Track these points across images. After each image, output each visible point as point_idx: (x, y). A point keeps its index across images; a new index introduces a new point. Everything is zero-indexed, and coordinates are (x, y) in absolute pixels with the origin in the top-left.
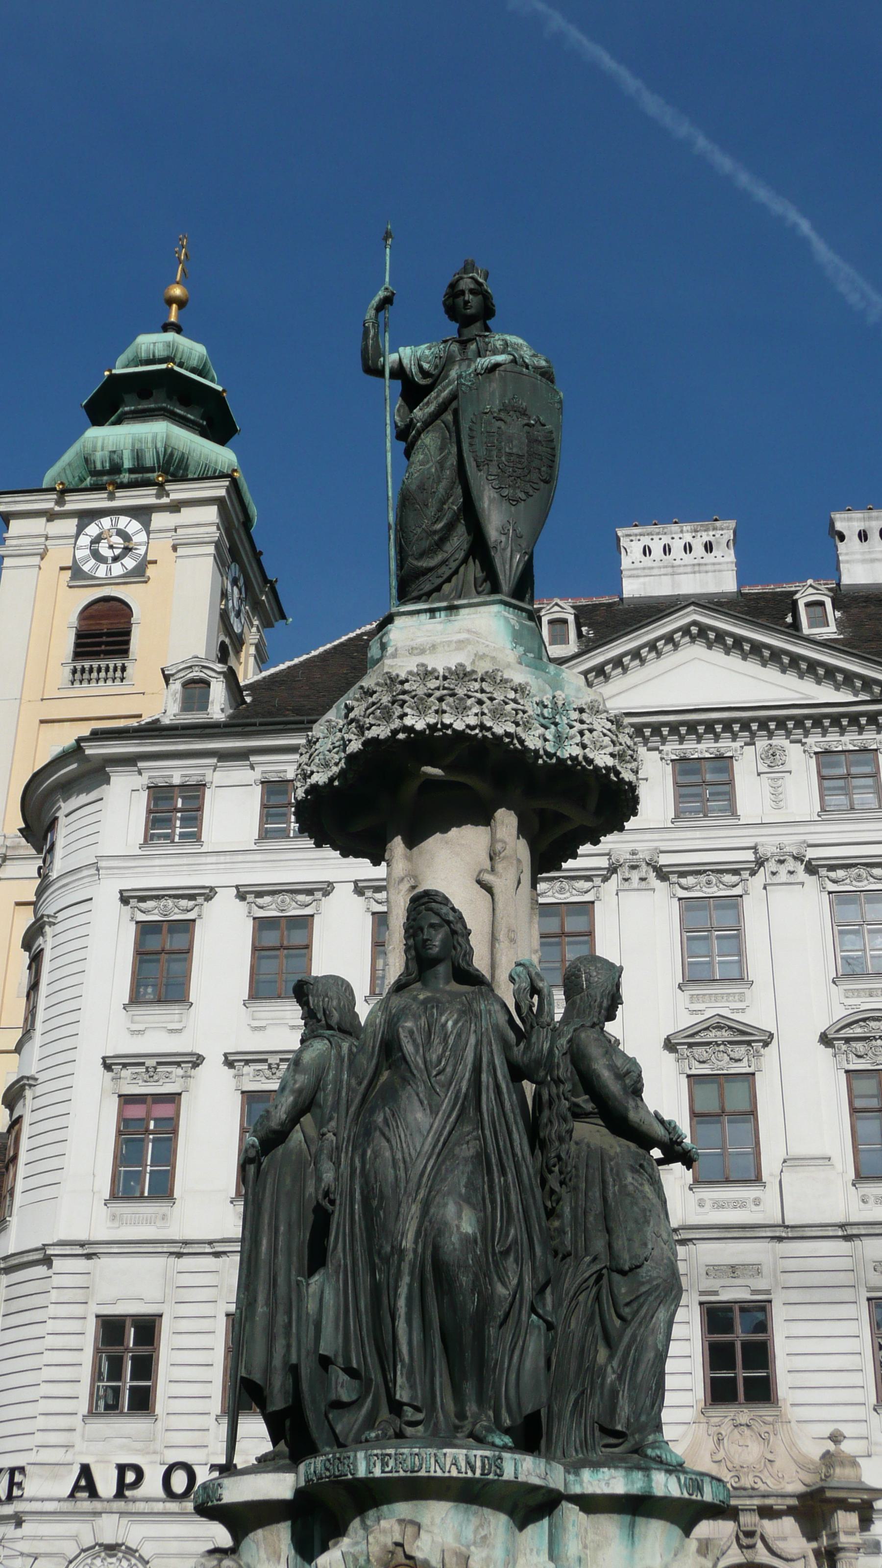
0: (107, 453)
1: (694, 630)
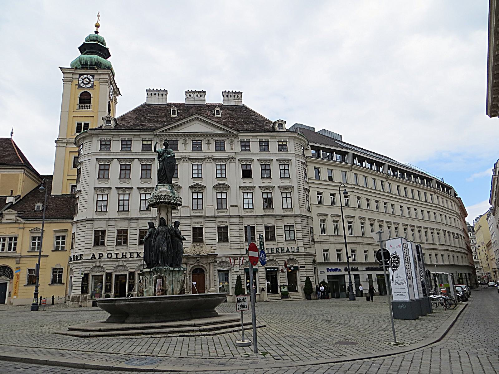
1: (197, 118)
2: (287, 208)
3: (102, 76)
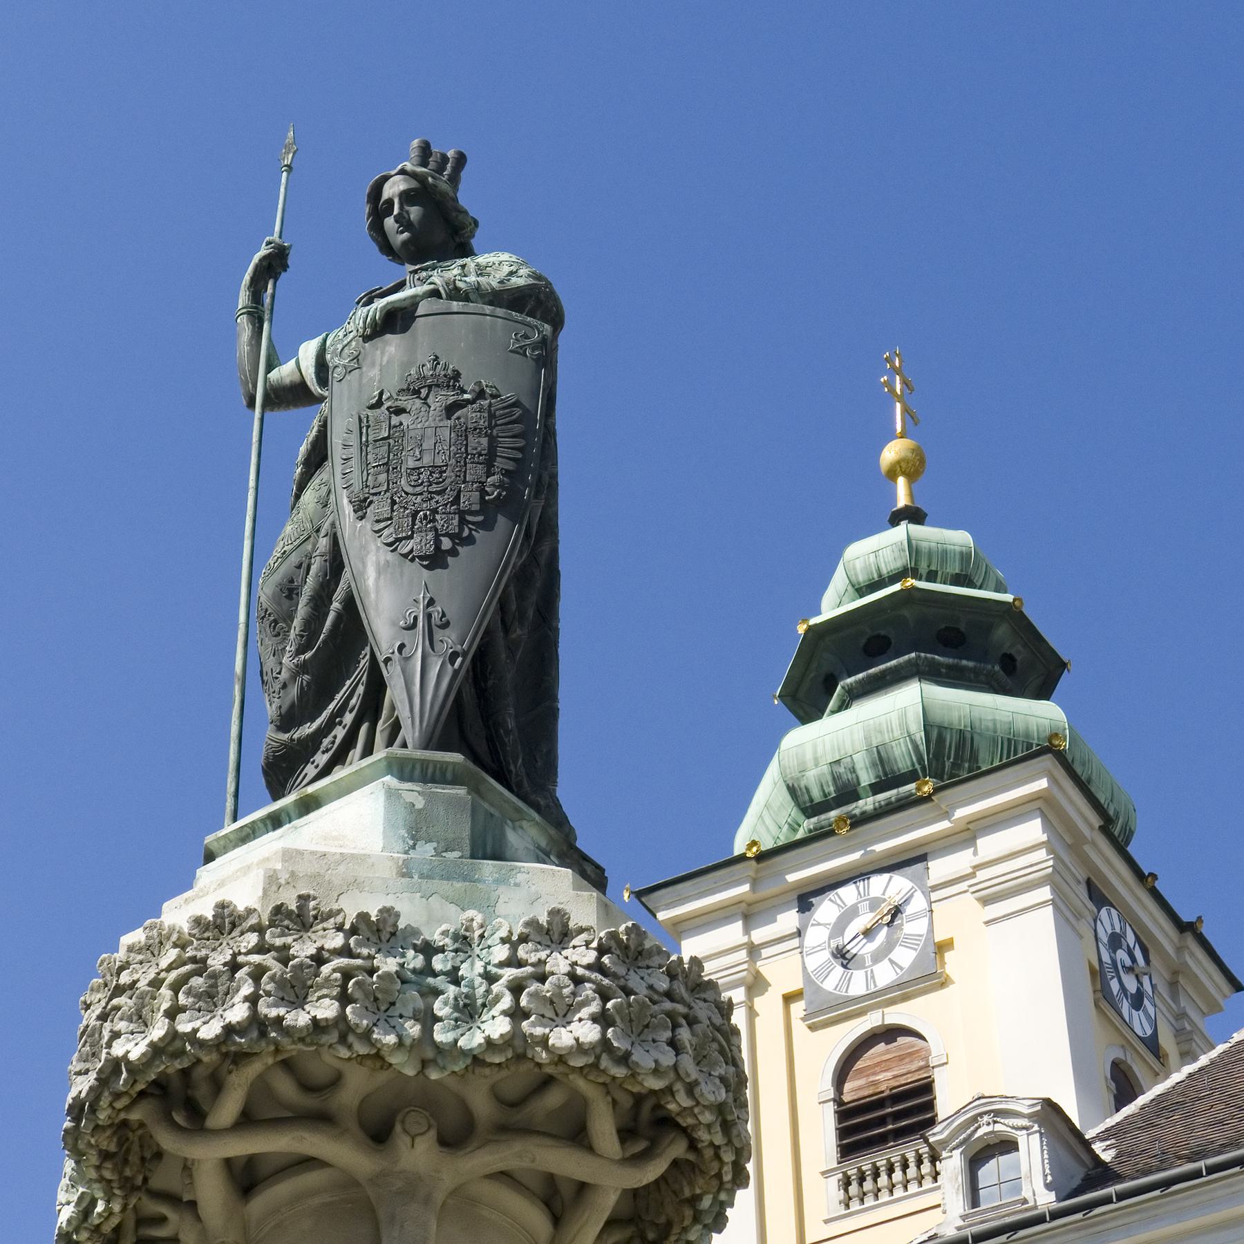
0: (825, 769)
3: (991, 845)
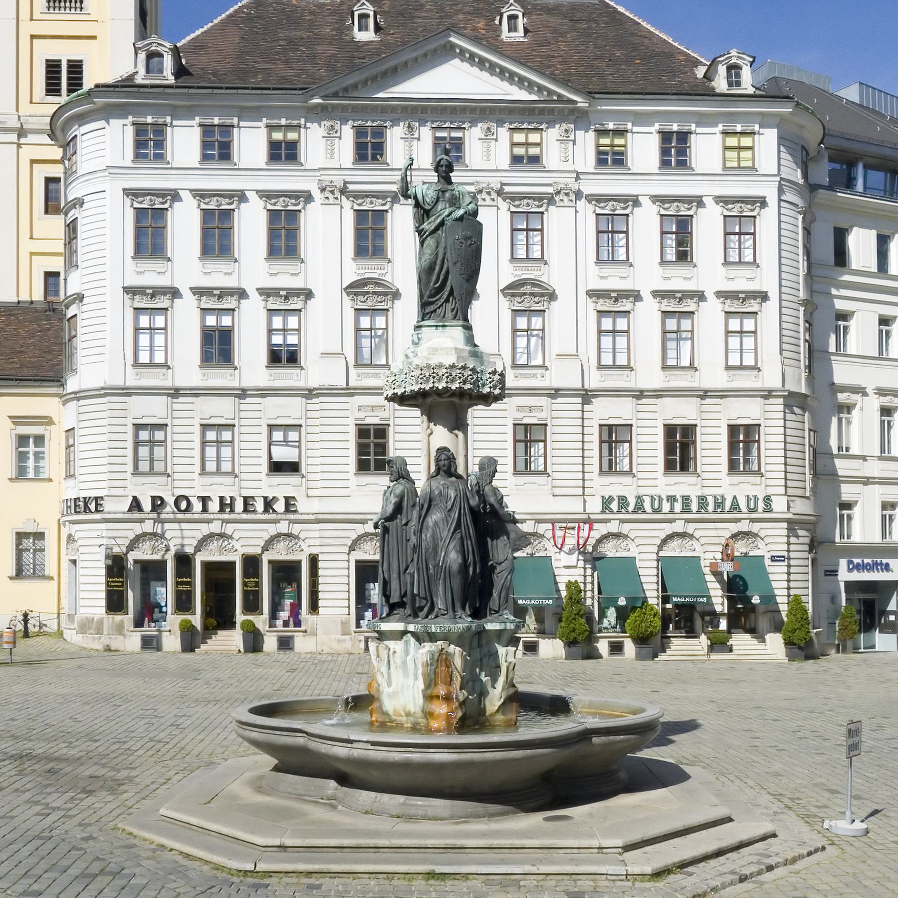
2: (741, 367)
